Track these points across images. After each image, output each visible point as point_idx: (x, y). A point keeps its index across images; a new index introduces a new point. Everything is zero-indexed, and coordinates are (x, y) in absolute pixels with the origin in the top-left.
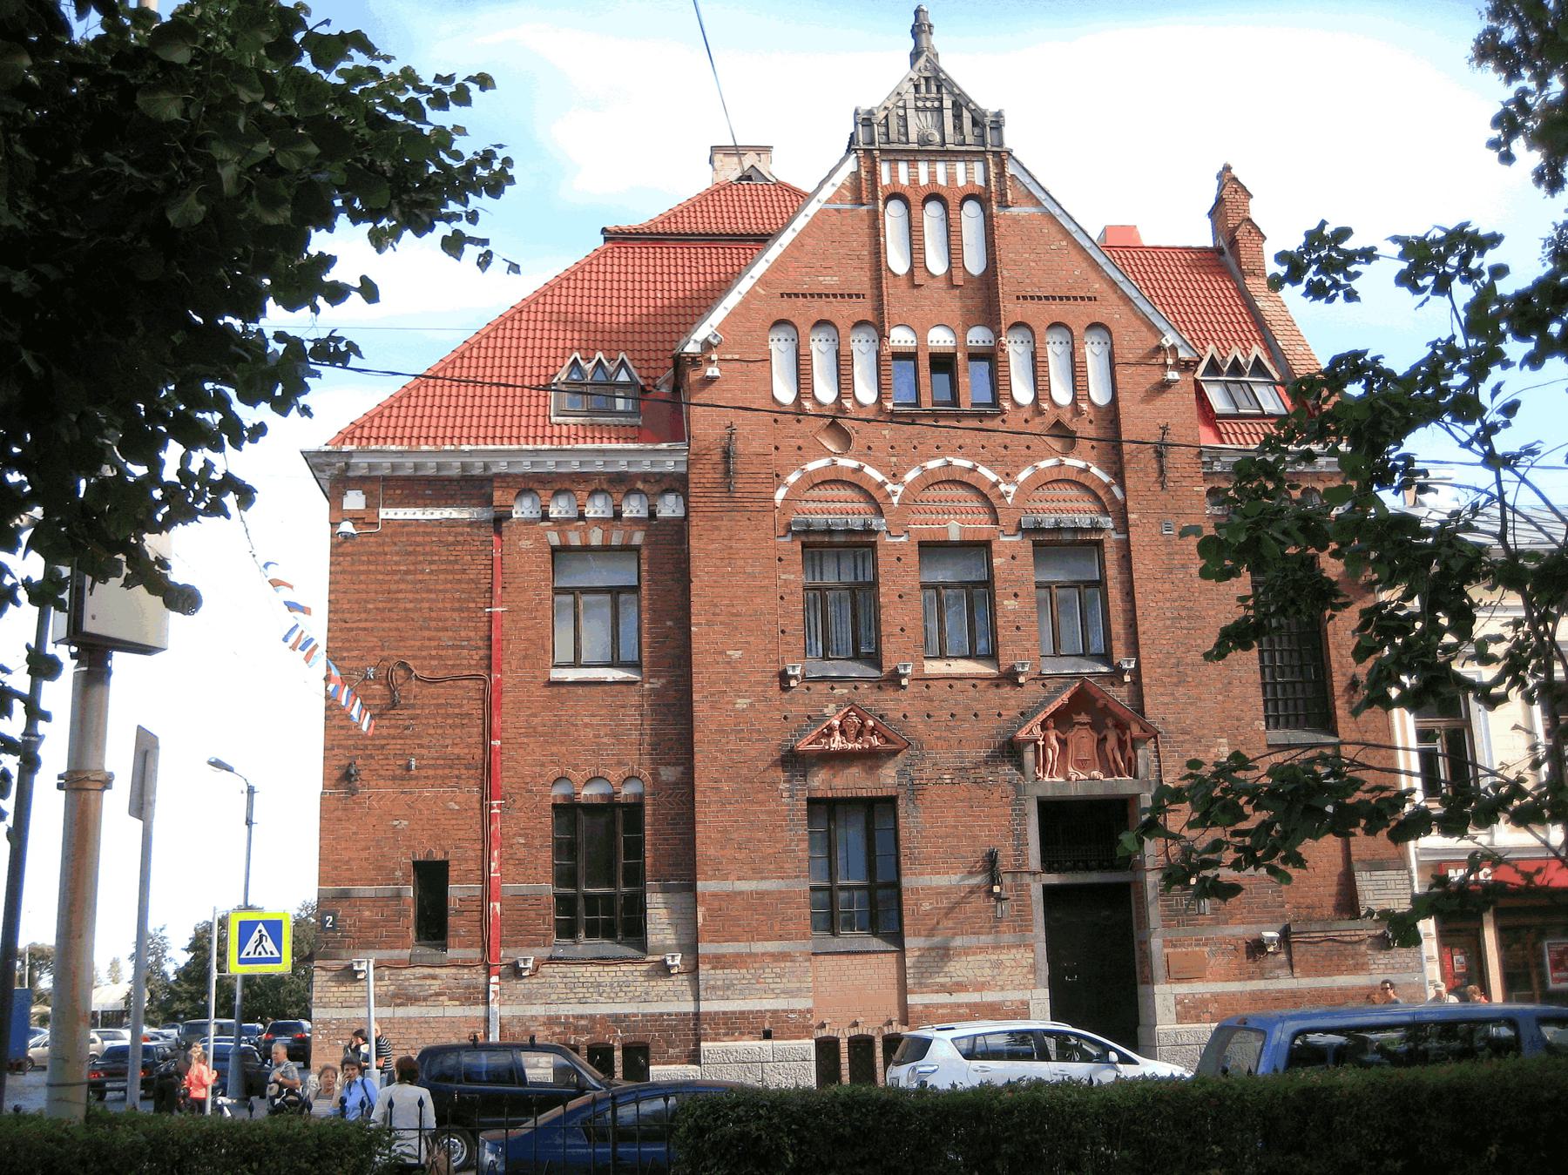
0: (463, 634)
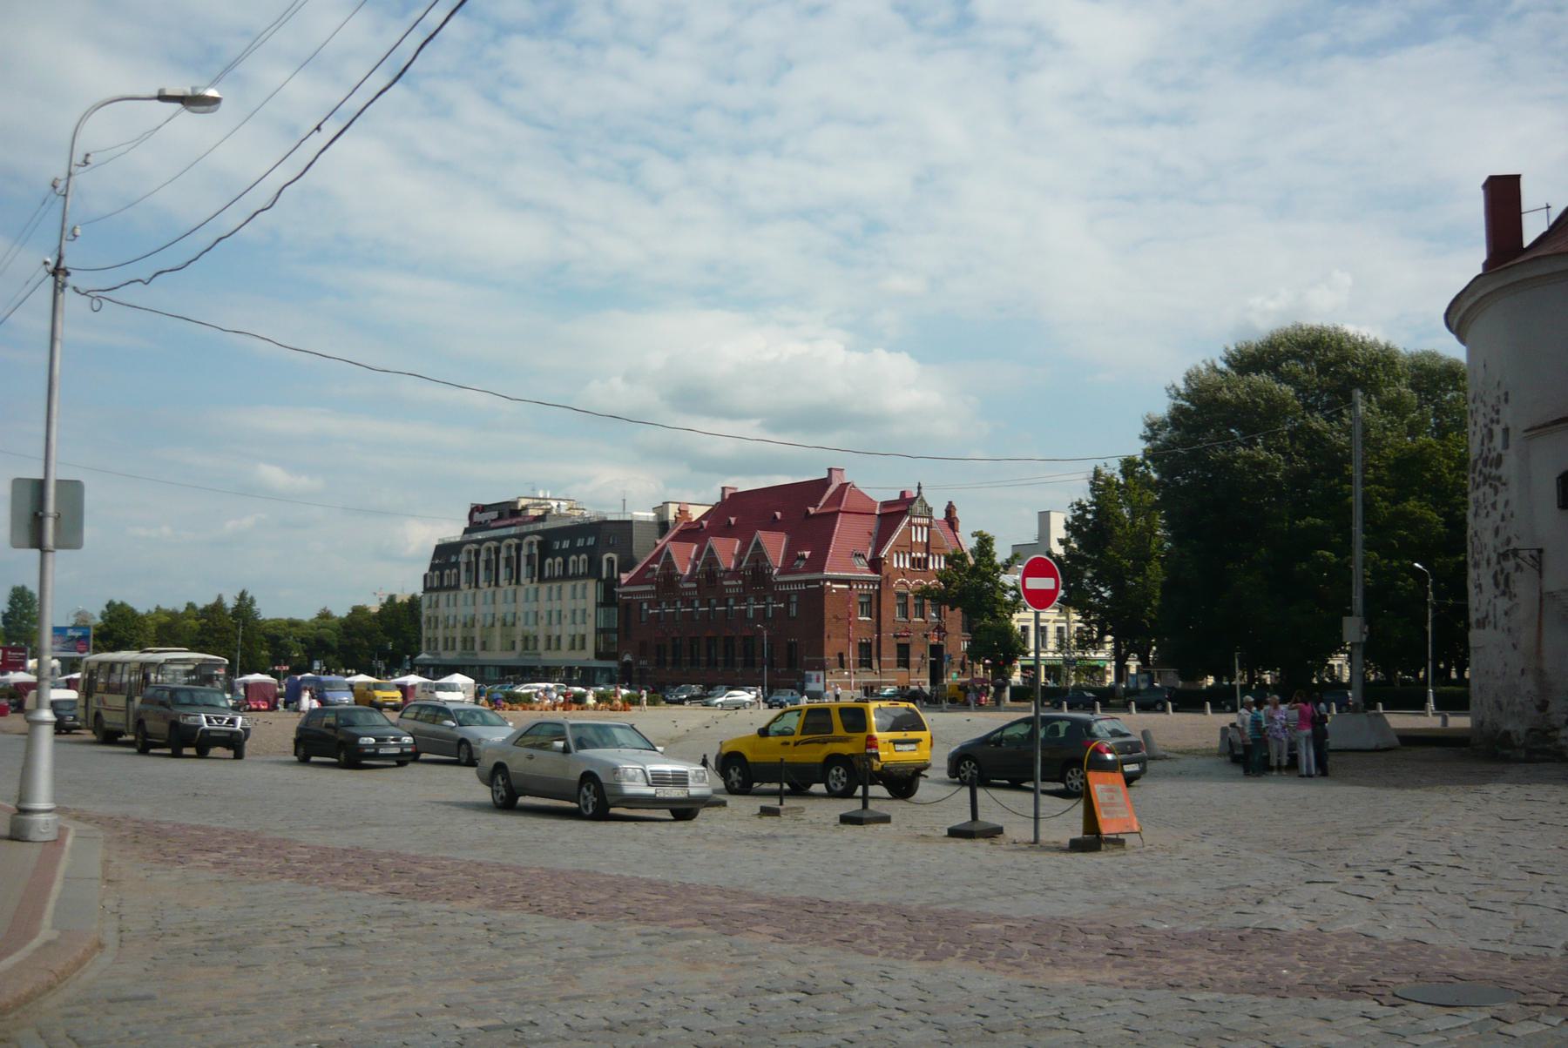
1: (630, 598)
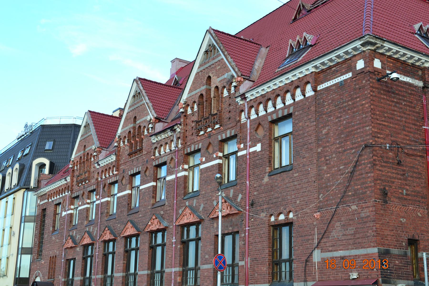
0: (416, 136)
1: (46, 201)
